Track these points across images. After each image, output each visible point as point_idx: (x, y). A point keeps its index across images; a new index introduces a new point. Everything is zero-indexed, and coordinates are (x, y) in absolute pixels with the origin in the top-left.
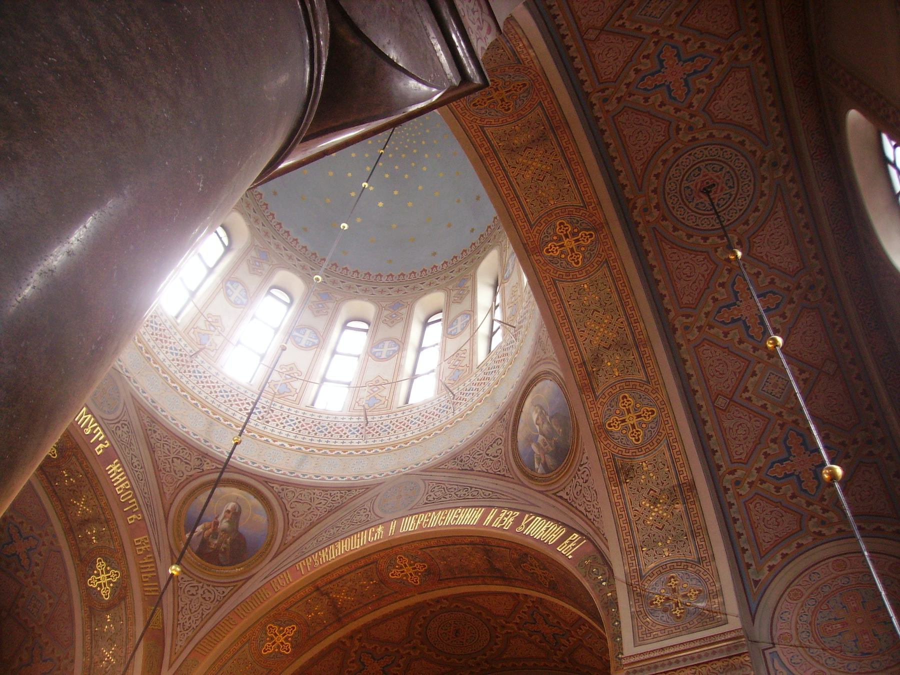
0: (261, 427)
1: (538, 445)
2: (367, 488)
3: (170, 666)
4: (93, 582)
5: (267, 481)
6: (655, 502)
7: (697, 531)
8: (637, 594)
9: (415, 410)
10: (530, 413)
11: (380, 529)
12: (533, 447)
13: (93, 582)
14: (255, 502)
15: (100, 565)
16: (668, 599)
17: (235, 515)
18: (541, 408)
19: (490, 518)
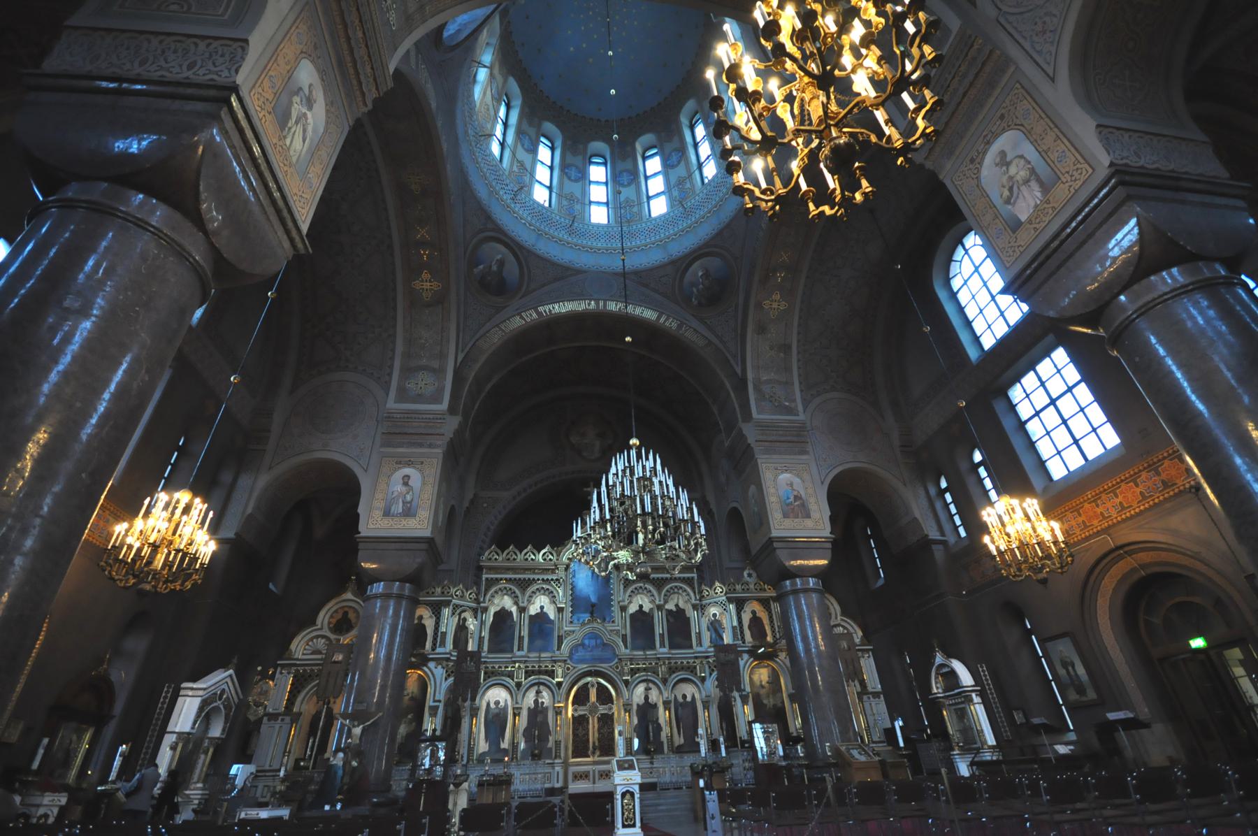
0: (513, 205)
1: (698, 290)
2: (578, 272)
3: (463, 351)
4: (417, 285)
5: (521, 247)
6: (771, 348)
7: (788, 369)
8: (756, 388)
9: (601, 229)
10: (697, 271)
11: (593, 302)
12: (695, 290)
13: (417, 285)
14: (512, 258)
15: (425, 275)
16: (771, 397)
17: (501, 263)
18: (707, 271)
19: (662, 320)
